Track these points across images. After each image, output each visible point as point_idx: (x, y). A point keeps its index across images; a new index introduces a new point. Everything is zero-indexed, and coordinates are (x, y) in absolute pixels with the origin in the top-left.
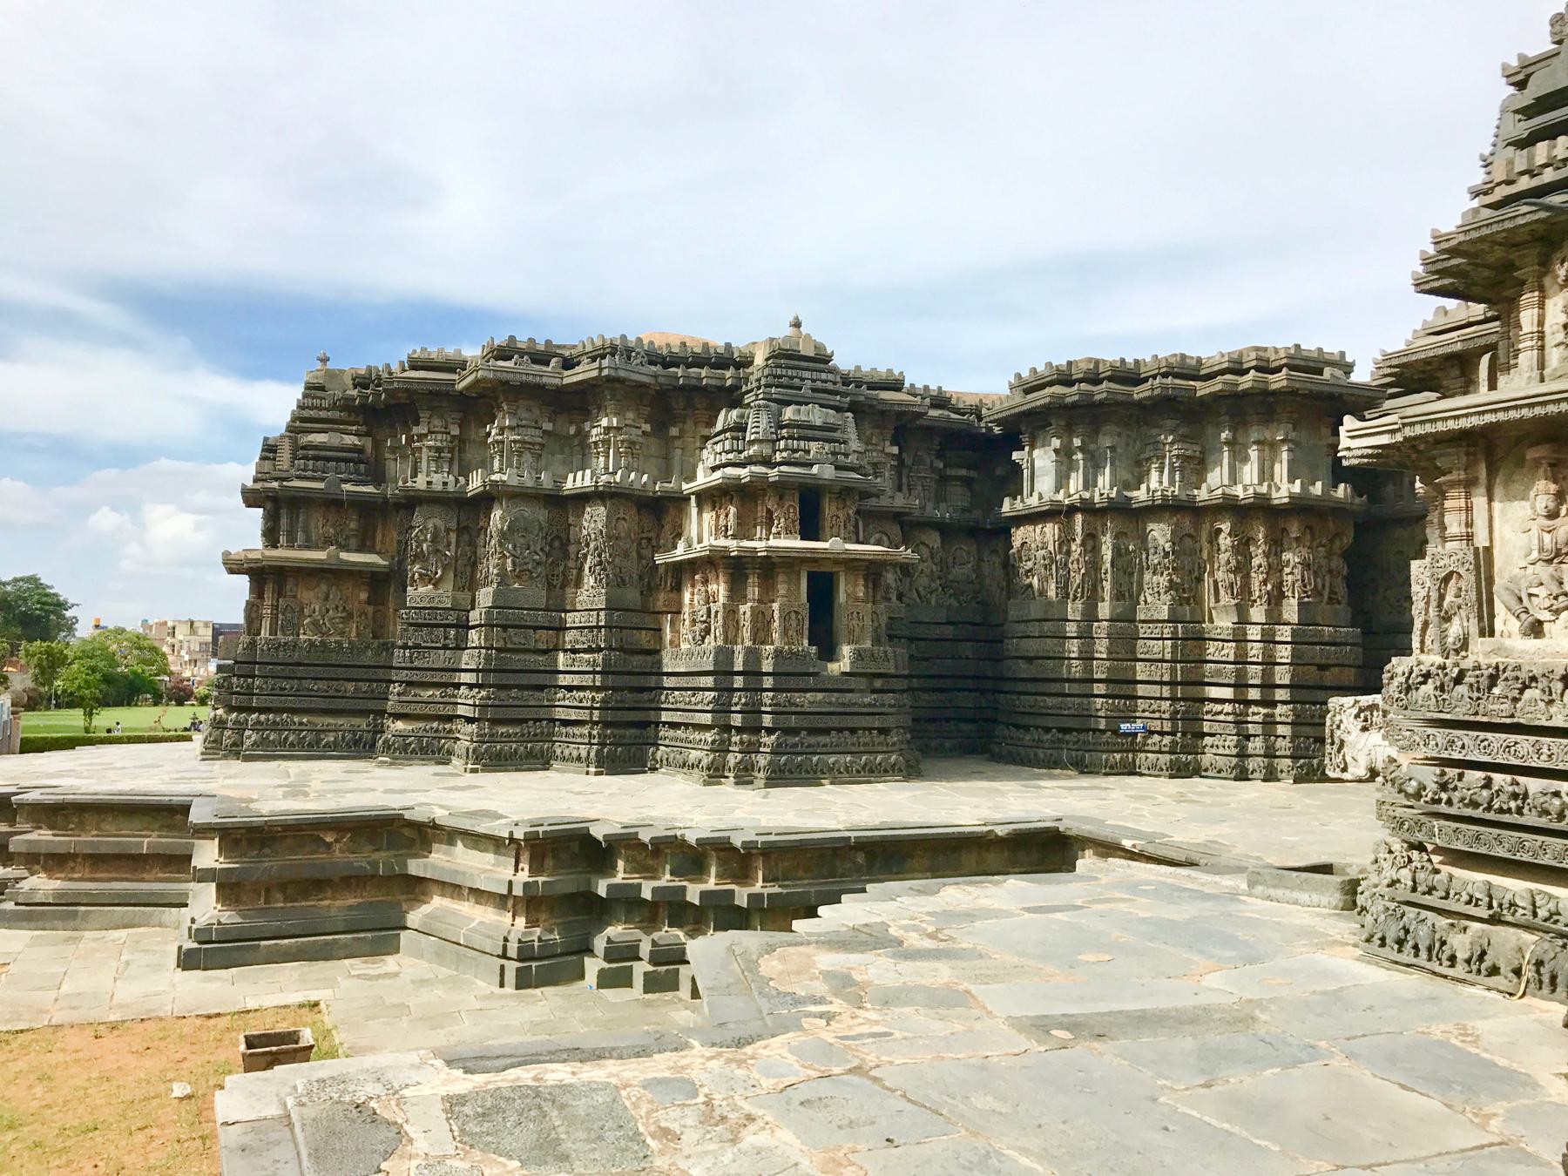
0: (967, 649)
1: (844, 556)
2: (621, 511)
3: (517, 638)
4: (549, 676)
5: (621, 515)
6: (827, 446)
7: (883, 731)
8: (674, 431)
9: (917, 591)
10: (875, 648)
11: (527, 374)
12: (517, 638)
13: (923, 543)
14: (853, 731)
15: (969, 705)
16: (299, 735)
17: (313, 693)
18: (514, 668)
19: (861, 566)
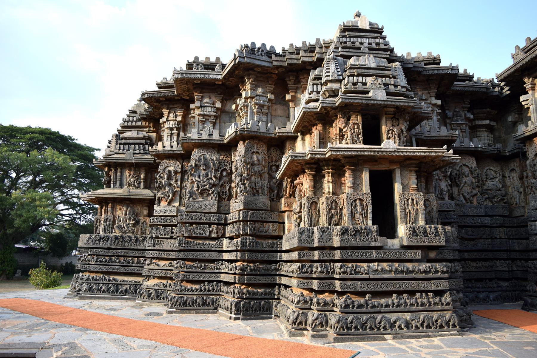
0: (500, 233)
1: (396, 154)
2: (255, 148)
3: (198, 231)
4: (217, 253)
5: (255, 150)
6: (380, 80)
7: (439, 293)
8: (288, 97)
9: (464, 197)
10: (427, 226)
11: (201, 74)
12: (198, 231)
13: (465, 165)
14: (412, 293)
15: (505, 269)
16: (108, 286)
17: (116, 264)
18: (196, 248)
19: (412, 164)
